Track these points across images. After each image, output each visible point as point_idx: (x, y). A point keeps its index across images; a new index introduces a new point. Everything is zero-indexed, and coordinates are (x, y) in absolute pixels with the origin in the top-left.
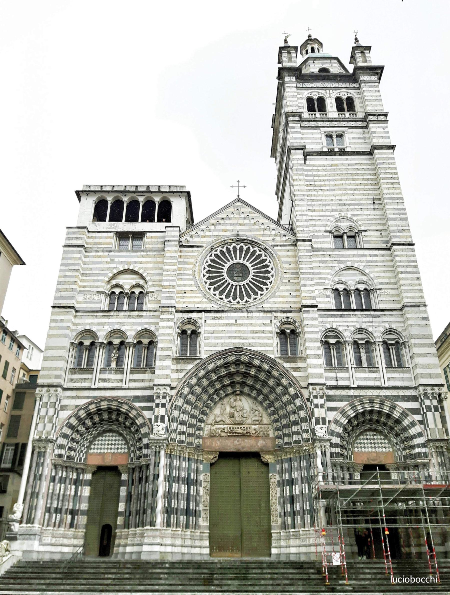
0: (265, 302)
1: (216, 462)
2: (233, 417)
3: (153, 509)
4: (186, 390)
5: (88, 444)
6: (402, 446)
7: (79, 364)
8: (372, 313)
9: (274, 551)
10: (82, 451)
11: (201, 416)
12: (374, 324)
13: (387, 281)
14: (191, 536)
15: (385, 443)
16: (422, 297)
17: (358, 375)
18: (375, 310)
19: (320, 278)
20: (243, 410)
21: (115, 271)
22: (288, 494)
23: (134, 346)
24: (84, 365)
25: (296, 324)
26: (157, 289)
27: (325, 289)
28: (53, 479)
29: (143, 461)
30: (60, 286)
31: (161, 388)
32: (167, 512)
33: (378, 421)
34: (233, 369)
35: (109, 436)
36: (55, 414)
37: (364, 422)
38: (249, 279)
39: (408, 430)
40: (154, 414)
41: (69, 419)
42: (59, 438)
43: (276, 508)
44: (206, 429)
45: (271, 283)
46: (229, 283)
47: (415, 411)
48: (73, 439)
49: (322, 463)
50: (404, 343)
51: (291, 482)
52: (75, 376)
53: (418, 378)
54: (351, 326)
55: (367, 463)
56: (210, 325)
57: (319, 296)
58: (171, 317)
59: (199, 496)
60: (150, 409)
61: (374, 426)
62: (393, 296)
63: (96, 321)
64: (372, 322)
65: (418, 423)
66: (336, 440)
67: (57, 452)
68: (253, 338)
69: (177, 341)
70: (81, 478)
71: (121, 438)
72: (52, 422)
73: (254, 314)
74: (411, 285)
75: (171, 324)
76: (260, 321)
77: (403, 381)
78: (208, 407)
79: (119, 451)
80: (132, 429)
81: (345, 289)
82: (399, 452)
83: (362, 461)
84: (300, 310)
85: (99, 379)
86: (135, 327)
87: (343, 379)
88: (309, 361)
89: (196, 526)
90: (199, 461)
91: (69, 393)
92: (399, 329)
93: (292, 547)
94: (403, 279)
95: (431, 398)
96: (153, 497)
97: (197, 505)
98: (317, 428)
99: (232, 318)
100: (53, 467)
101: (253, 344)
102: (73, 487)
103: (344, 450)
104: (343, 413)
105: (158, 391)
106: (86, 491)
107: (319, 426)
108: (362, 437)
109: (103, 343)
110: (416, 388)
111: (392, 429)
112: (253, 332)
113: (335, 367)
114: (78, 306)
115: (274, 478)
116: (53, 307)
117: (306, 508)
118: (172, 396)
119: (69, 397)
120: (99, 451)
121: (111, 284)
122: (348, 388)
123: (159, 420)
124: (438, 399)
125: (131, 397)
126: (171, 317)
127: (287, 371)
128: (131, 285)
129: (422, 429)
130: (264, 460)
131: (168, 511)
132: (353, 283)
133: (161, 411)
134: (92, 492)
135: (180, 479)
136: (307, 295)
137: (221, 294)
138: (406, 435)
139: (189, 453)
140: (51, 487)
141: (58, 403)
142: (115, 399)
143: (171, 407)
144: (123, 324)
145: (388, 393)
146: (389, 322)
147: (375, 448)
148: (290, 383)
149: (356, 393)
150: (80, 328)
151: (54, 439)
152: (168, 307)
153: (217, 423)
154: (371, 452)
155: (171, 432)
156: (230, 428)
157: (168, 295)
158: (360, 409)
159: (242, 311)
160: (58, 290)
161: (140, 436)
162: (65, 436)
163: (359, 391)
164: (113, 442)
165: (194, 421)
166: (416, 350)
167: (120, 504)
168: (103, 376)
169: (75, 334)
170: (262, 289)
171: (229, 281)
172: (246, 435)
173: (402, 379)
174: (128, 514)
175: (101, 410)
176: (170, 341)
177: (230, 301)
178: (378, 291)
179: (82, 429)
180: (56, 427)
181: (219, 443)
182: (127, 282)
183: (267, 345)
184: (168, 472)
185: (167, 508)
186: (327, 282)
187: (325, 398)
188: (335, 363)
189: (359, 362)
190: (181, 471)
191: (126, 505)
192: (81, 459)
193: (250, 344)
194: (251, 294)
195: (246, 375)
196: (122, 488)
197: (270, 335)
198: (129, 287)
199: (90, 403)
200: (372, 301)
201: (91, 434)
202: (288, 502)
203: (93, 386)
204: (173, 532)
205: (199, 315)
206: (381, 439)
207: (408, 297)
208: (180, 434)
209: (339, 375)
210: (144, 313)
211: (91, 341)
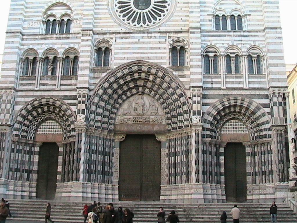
0: (162, 25)
1: (124, 141)
2: (136, 110)
3: (78, 170)
4: (101, 92)
5: (36, 128)
6: (255, 130)
7: (27, 74)
8: (242, 33)
9: (162, 198)
10: (32, 133)
11: (113, 110)
12: (243, 42)
13: (255, 9)
14: (105, 187)
16: (279, 22)
17: (228, 80)
18: (244, 31)
19: (205, 7)
20: (144, 105)
21: (50, 4)
22: (173, 162)
23: (64, 60)
24: (29, 74)
25: (185, 42)
26: (80, 16)
27: (208, 15)
28: (13, 150)
29: (72, 140)
30: (11, 17)
31: (82, 90)
32: (88, 172)
34: (136, 76)
35: (50, 123)
36: (11, 107)
37: (230, 113)
38: (151, 7)
40: (77, 108)
41: (21, 111)
42: (15, 124)
43: (165, 171)
44: (117, 118)
45: (167, 10)
46: (135, 12)
47: (266, 106)
48: (25, 125)
49: (195, 141)
50: (263, 56)
51: (175, 154)
52: (24, 82)
53: (270, 82)
54: (225, 43)
55: (230, 141)
56: (119, 44)
57: (204, 20)
58: (90, 38)
59: (112, 162)
60: (74, 104)
61: (237, 116)
62: (258, 21)
63: (37, 42)
64: (241, 41)
65: (267, 114)
66: (208, 126)
67: (15, 133)
68: (152, 53)
69: (95, 56)
70: (32, 150)
71: (58, 124)
72: (9, 113)
73: (153, 35)
74: (272, 12)
75: (89, 43)
76: (158, 40)
78: (118, 104)
79: (57, 132)
80: (64, 118)
81: (223, 15)
82: (252, 134)
84: (188, 31)
85: (40, 84)
86: (63, 46)
87: (216, 83)
88: (192, 70)
89: (110, 181)
90: (111, 140)
91: (20, 93)
92: (261, 46)
93: (173, 195)
94: (266, 7)
95: (277, 96)
96: (77, 163)
97: (110, 168)
98: (194, 117)
99: (136, 37)
100: (12, 142)
101: (151, 58)
102: (28, 156)
103: (213, 133)
104: (215, 107)
105: (80, 92)
106: (36, 158)
107: (195, 116)
108: (227, 124)
109: (42, 58)
110: (268, 89)
112: (152, 48)
114: (24, 31)
115: (164, 151)
116: (7, 33)
117: (184, 171)
118: (90, 96)
119: (20, 96)
120: (43, 132)
121: (47, 14)
122: (219, 89)
123: (81, 112)
124: (282, 97)
125: (62, 96)
126: (90, 38)
127: (176, 77)
128: (61, 14)
129: (269, 118)
130: (158, 140)
131: (88, 172)
132: (230, 11)
133: (83, 106)
134: (39, 158)
135: (98, 152)
136: (194, 20)
137: (128, 19)
138: (258, 123)
139: (104, 134)
140: (12, 156)
141: (13, 100)
142: (52, 97)
143: (90, 103)
144: (56, 44)
145: (248, 92)
146: (254, 41)
147: (236, 131)
148: (177, 86)
149: (225, 92)
150: (26, 48)
151: (12, 124)
152: (87, 30)
153: (125, 114)
154: (234, 133)
155: (90, 121)
156: (134, 118)
157: (87, 21)
158: (227, 104)
159: (144, 33)
160: (10, 20)
161: (69, 123)
162: (20, 123)
163: (227, 91)
164: (53, 127)
165: (107, 113)
166: (271, 61)
167: (58, 167)
168: (42, 82)
169: (22, 52)
170: (160, 16)
171: (135, 9)
172: (146, 122)
173: (259, 83)
174: (64, 173)
175: (42, 105)
176: (88, 56)
177: (135, 25)
178: (248, 16)
179: (30, 117)
180: (12, 116)
181: (126, 128)
182: (58, 12)
183: (162, 58)
184: (88, 147)
185: (88, 170)
186: (210, 9)
187: (201, 97)
188: (212, 70)
189: (229, 71)
190: (98, 147)
191: (62, 168)
192: (31, 138)
193: (148, 57)
194: (152, 19)
195: (146, 80)
196: (59, 157)
197: (165, 51)
198: (60, 16)
199: (35, 101)
200: (243, 24)
201: (37, 121)
202: (173, 167)
203: (36, 89)
204: (92, 185)
205: (111, 36)
206: (241, 125)
207: (268, 22)
208: (97, 121)
209: (214, 80)
210: (71, 36)
211: (34, 56)
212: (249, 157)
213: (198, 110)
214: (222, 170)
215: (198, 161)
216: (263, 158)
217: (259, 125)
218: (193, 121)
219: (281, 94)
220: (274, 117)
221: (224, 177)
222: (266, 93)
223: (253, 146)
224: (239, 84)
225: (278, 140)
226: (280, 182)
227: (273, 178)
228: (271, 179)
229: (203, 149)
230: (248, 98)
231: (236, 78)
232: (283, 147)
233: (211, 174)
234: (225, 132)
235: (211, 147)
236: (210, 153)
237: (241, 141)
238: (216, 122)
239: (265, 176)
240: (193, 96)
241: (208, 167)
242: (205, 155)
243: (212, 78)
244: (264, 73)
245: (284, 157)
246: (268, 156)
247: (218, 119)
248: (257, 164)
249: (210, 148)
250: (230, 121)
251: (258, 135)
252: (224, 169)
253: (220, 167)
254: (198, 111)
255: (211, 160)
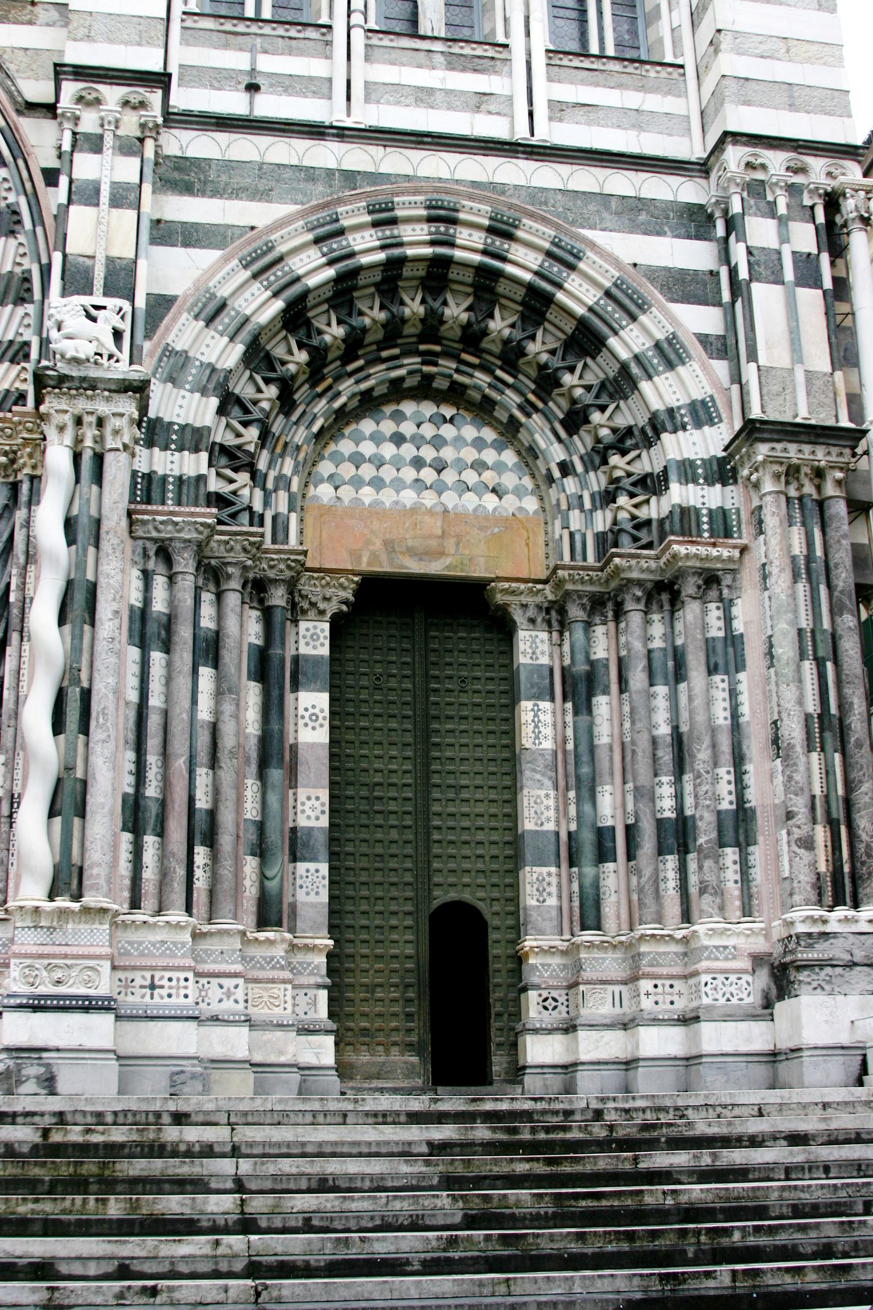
6: (597, 481)
15: (500, 467)
33: (472, 337)
39: (635, 386)
47: (688, 287)
49: (70, 525)
55: (385, 567)
65: (695, 349)
77: (639, 127)
83: (356, 555)
87: (289, 84)
103: (243, 478)
104: (264, 263)
108: (367, 426)
111: (547, 382)
113: (257, 20)
124: (821, 218)
138: (622, 421)
147: (439, 488)
158: (366, 246)
173: (637, 119)
206: (479, 444)
212: (545, 705)
213: (115, 253)
214: (312, 808)
215: (86, 696)
216: (661, 703)
217: (629, 442)
218: (54, 334)
219: (807, 202)
220: (762, 361)
221: (324, 868)
222: (688, 191)
223: (575, 612)
224: (478, 108)
225: (798, 548)
226: (820, 902)
227: (757, 874)
228: (733, 889)
229: (135, 598)
230: (543, 220)
231: (450, 67)
232: (835, 611)
233: (205, 830)
234: (347, 493)
235: (219, 596)
236: (209, 650)
237: (479, 571)
238: (272, 391)
239: (683, 869)
240: (74, 146)
241: (180, 764)
242: (157, 657)
243: (252, 50)
244: (669, 59)
245: (847, 691)
246: (709, 686)
247: (292, 368)
248: (609, 761)
249: (207, 611)
250: (388, 409)
251: (623, 515)
252: (324, 795)
253: (292, 781)
254: (110, 261)
255: (217, 712)
